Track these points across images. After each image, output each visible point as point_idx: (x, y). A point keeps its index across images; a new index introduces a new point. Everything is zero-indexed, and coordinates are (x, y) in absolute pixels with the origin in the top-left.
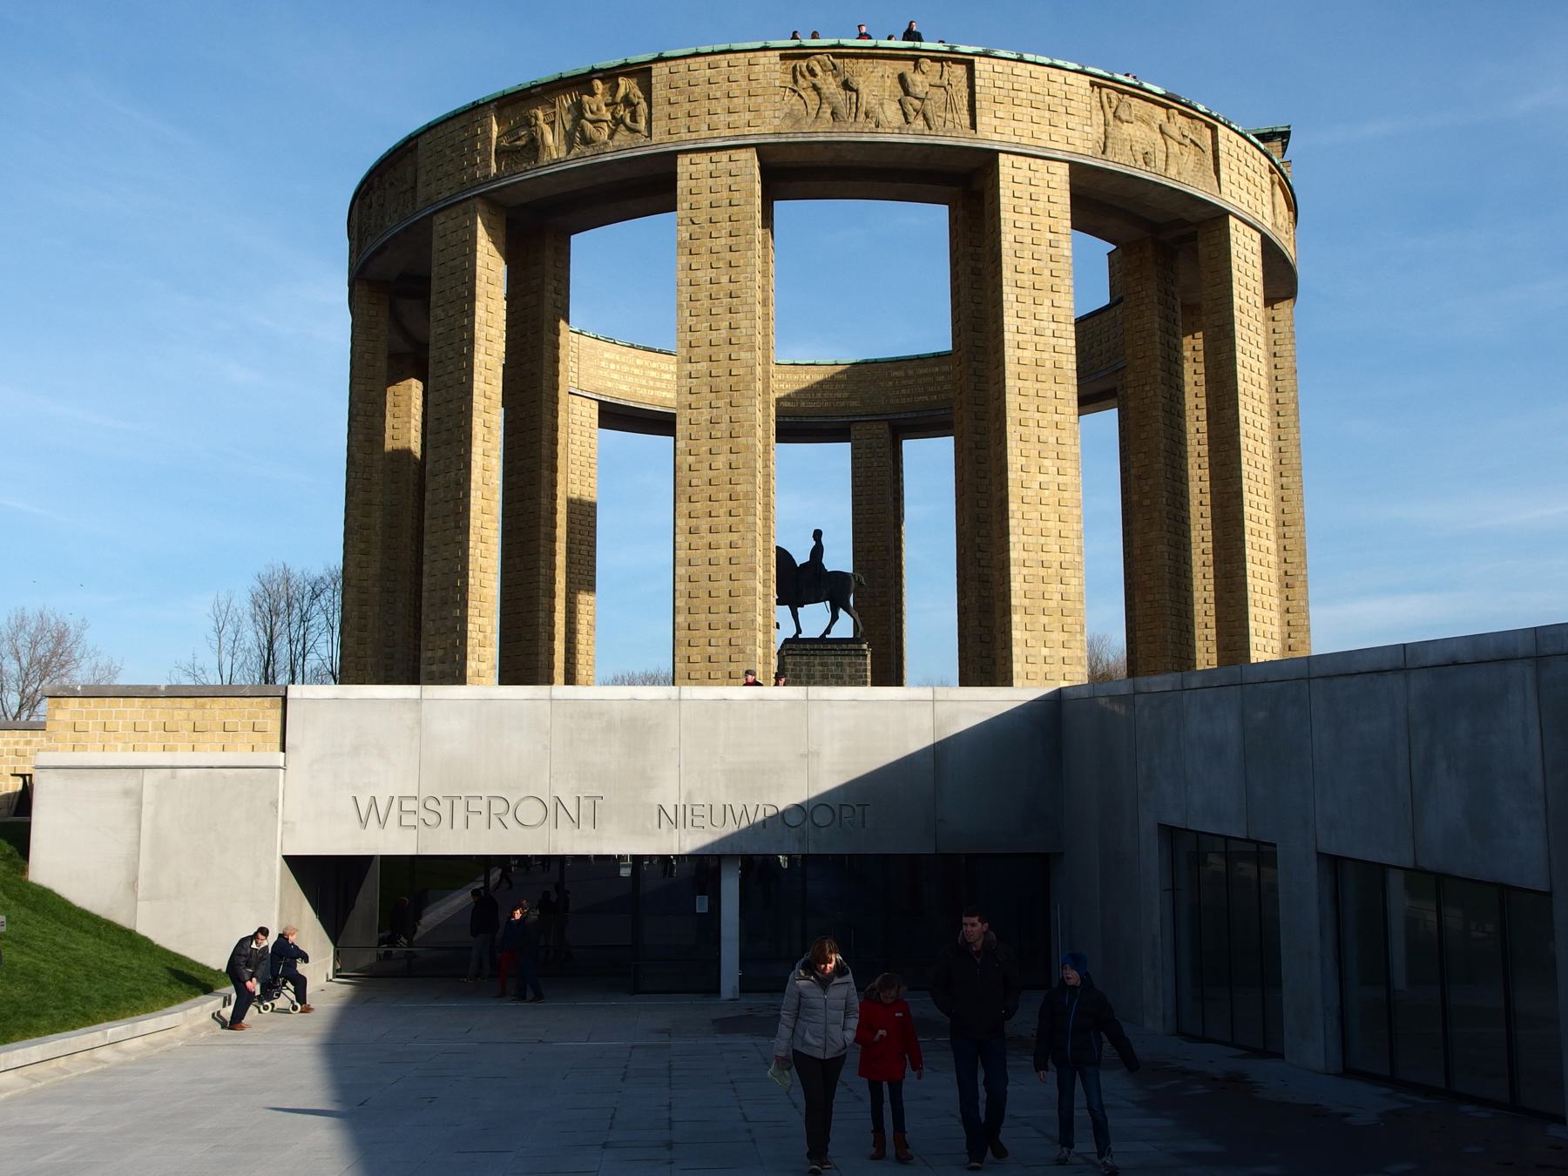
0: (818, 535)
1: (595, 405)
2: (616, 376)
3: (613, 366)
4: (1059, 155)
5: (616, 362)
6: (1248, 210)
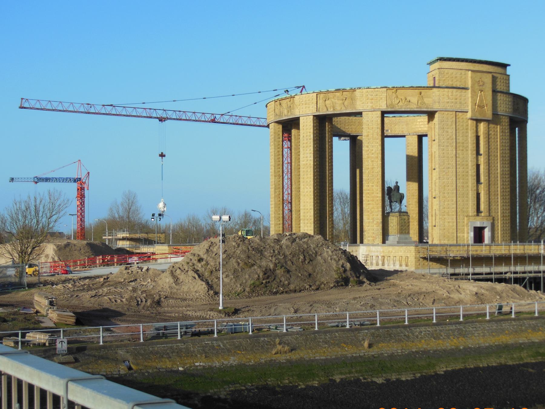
0: (397, 183)
1: (417, 136)
2: (422, 126)
3: (421, 123)
4: (310, 115)
5: (422, 122)
6: (371, 108)
